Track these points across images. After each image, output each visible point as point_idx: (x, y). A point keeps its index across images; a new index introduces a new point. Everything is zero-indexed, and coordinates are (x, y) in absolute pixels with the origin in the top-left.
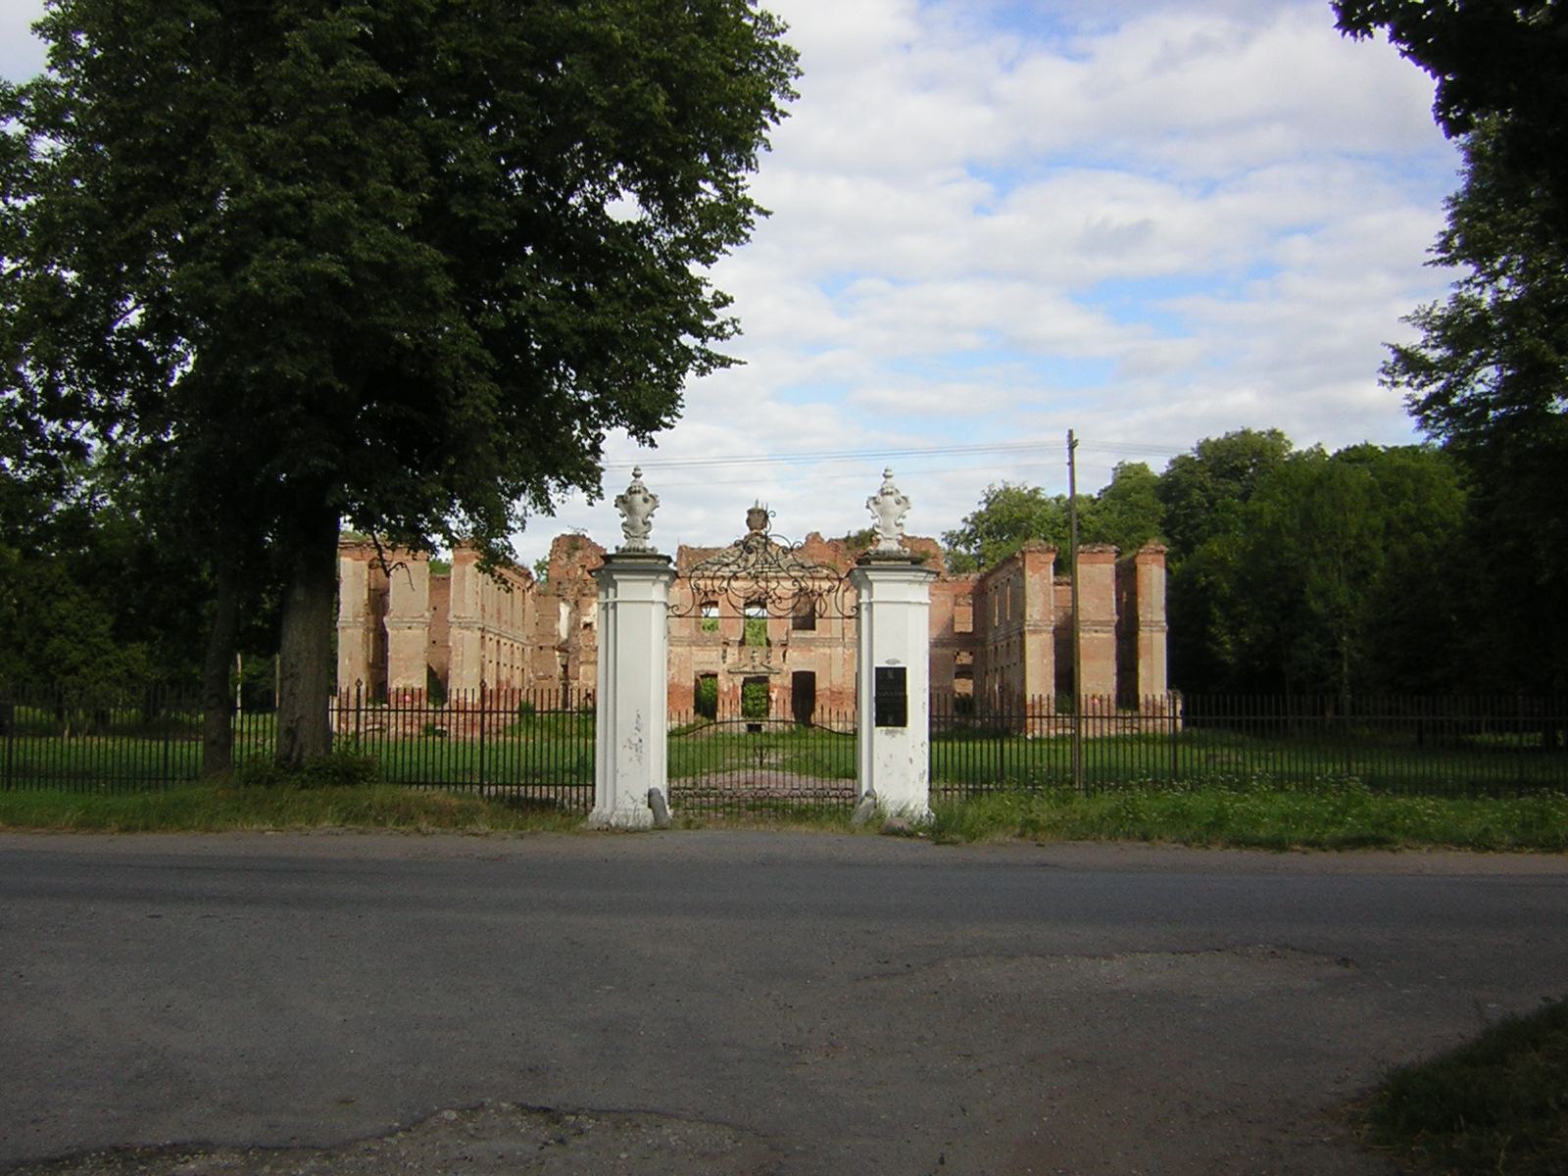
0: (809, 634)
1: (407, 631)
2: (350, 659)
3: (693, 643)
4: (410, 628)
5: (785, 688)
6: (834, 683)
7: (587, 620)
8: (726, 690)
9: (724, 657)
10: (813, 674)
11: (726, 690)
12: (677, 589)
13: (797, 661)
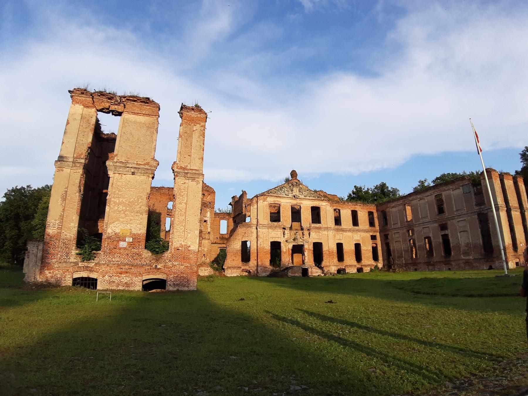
0: (318, 225)
1: (129, 177)
2: (64, 199)
3: (271, 227)
4: (133, 173)
5: (310, 250)
6: (330, 248)
7: (206, 219)
8: (285, 251)
9: (284, 234)
10: (321, 243)
11: (285, 251)
12: (262, 201)
13: (315, 237)
